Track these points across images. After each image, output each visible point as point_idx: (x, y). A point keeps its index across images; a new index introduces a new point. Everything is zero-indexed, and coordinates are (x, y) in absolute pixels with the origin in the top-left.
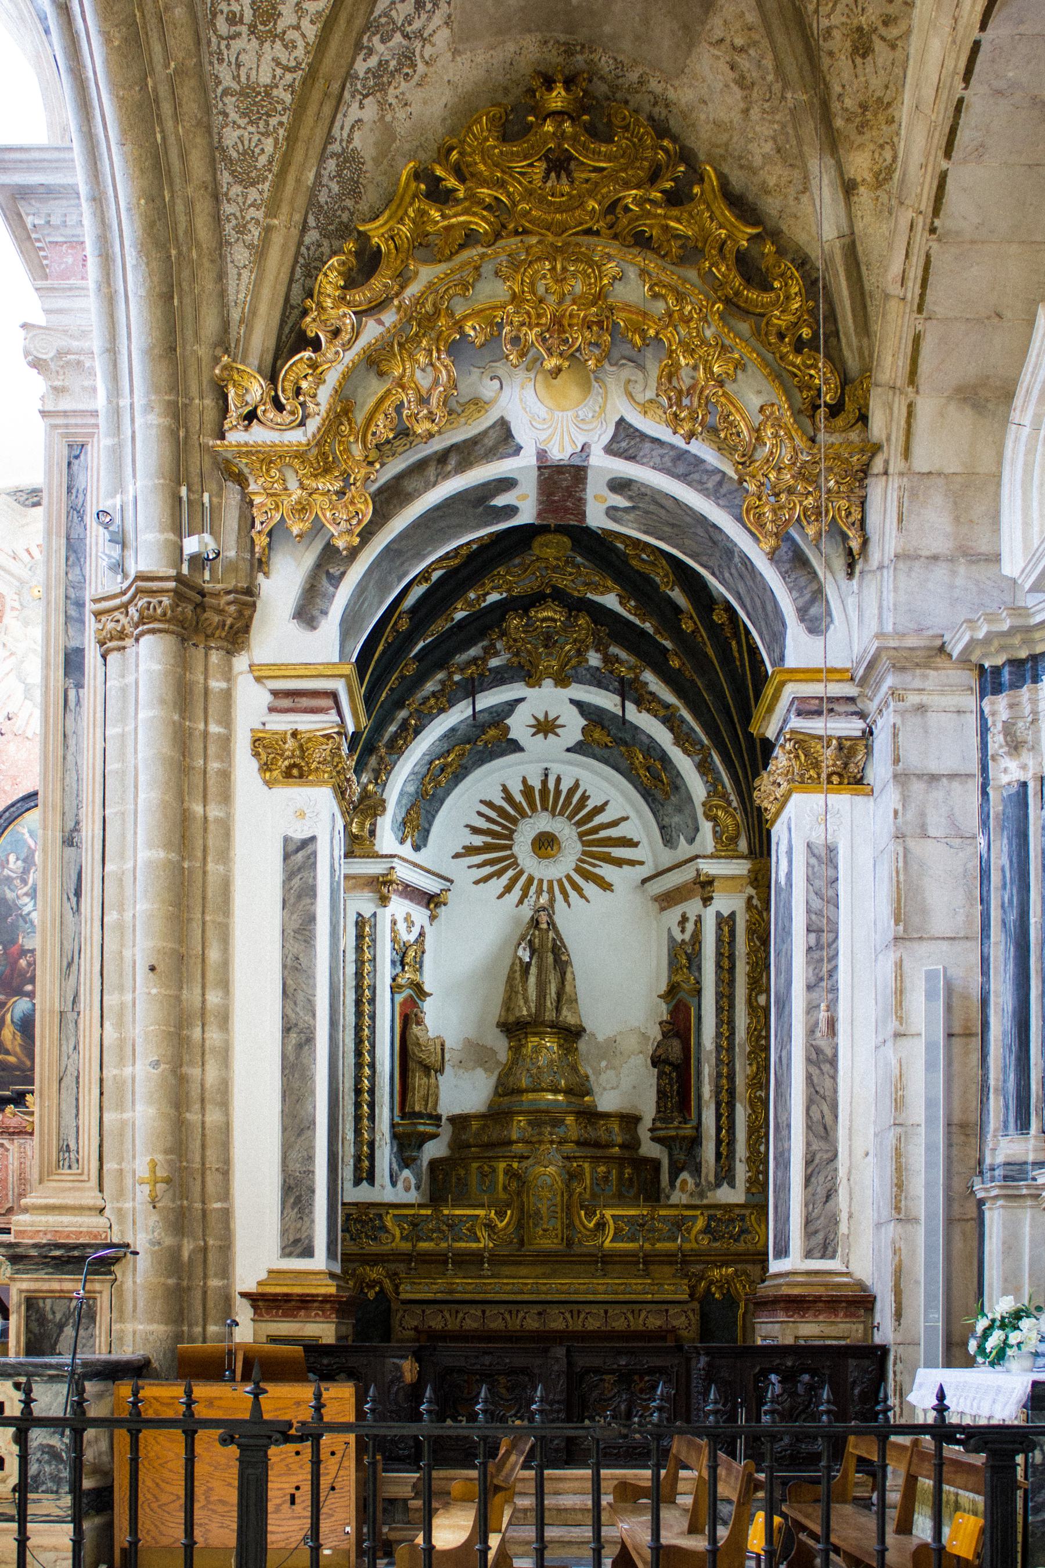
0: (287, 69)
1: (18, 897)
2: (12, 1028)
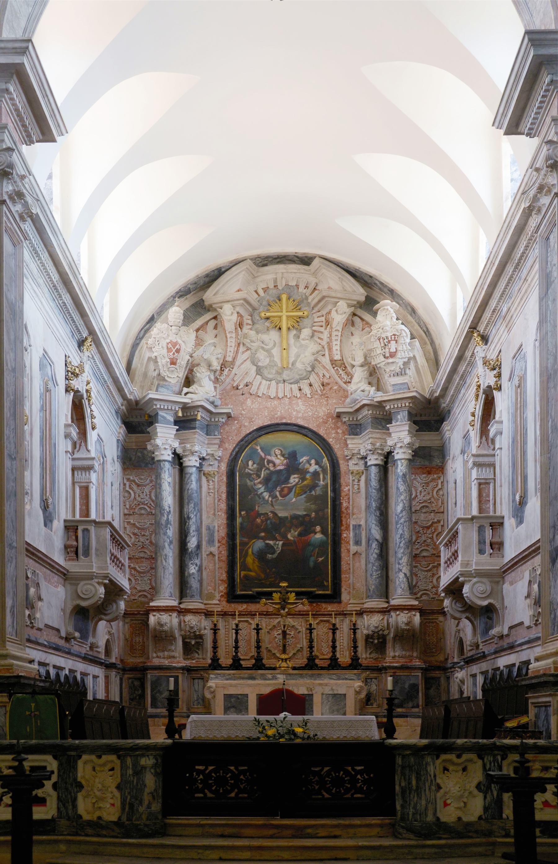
2: (252, 557)
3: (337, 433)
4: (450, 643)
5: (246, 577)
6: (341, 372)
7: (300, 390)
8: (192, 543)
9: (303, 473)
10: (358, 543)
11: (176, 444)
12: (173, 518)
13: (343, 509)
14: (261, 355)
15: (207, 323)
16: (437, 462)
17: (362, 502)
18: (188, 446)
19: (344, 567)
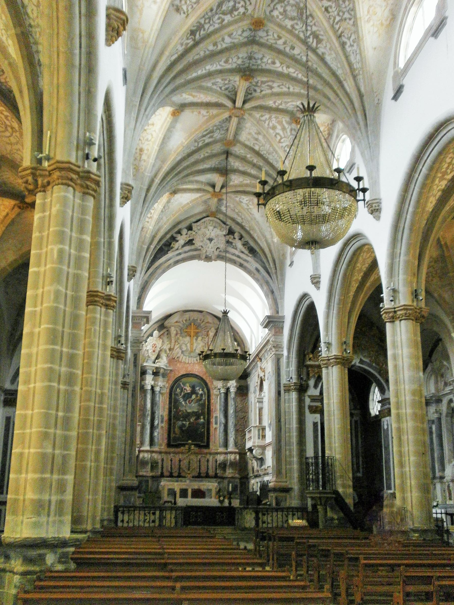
4: (250, 467)
9: (197, 394)
10: (216, 423)
16: (245, 391)
17: (218, 407)
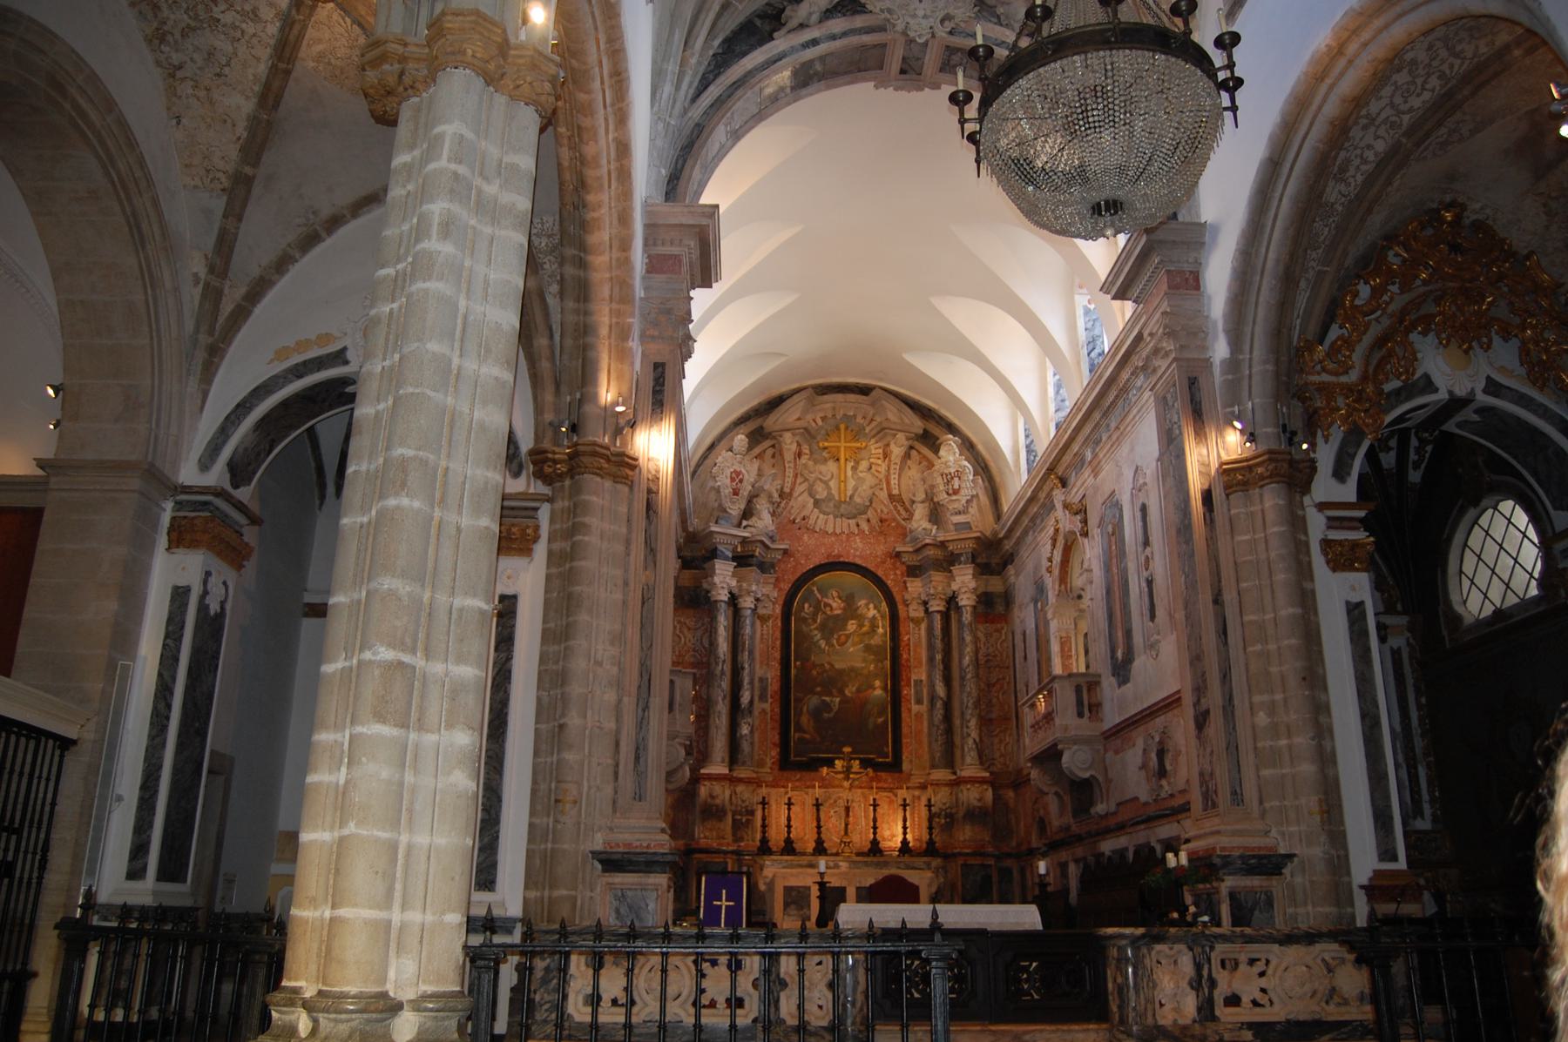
0: (1344, 196)
1: (811, 631)
3: (895, 574)
5: (801, 740)
6: (900, 508)
7: (858, 525)
8: (745, 698)
9: (860, 618)
11: (734, 583)
12: (727, 668)
13: (903, 662)
14: (819, 488)
15: (764, 451)
16: (1000, 609)
18: (744, 585)
19: (905, 730)
